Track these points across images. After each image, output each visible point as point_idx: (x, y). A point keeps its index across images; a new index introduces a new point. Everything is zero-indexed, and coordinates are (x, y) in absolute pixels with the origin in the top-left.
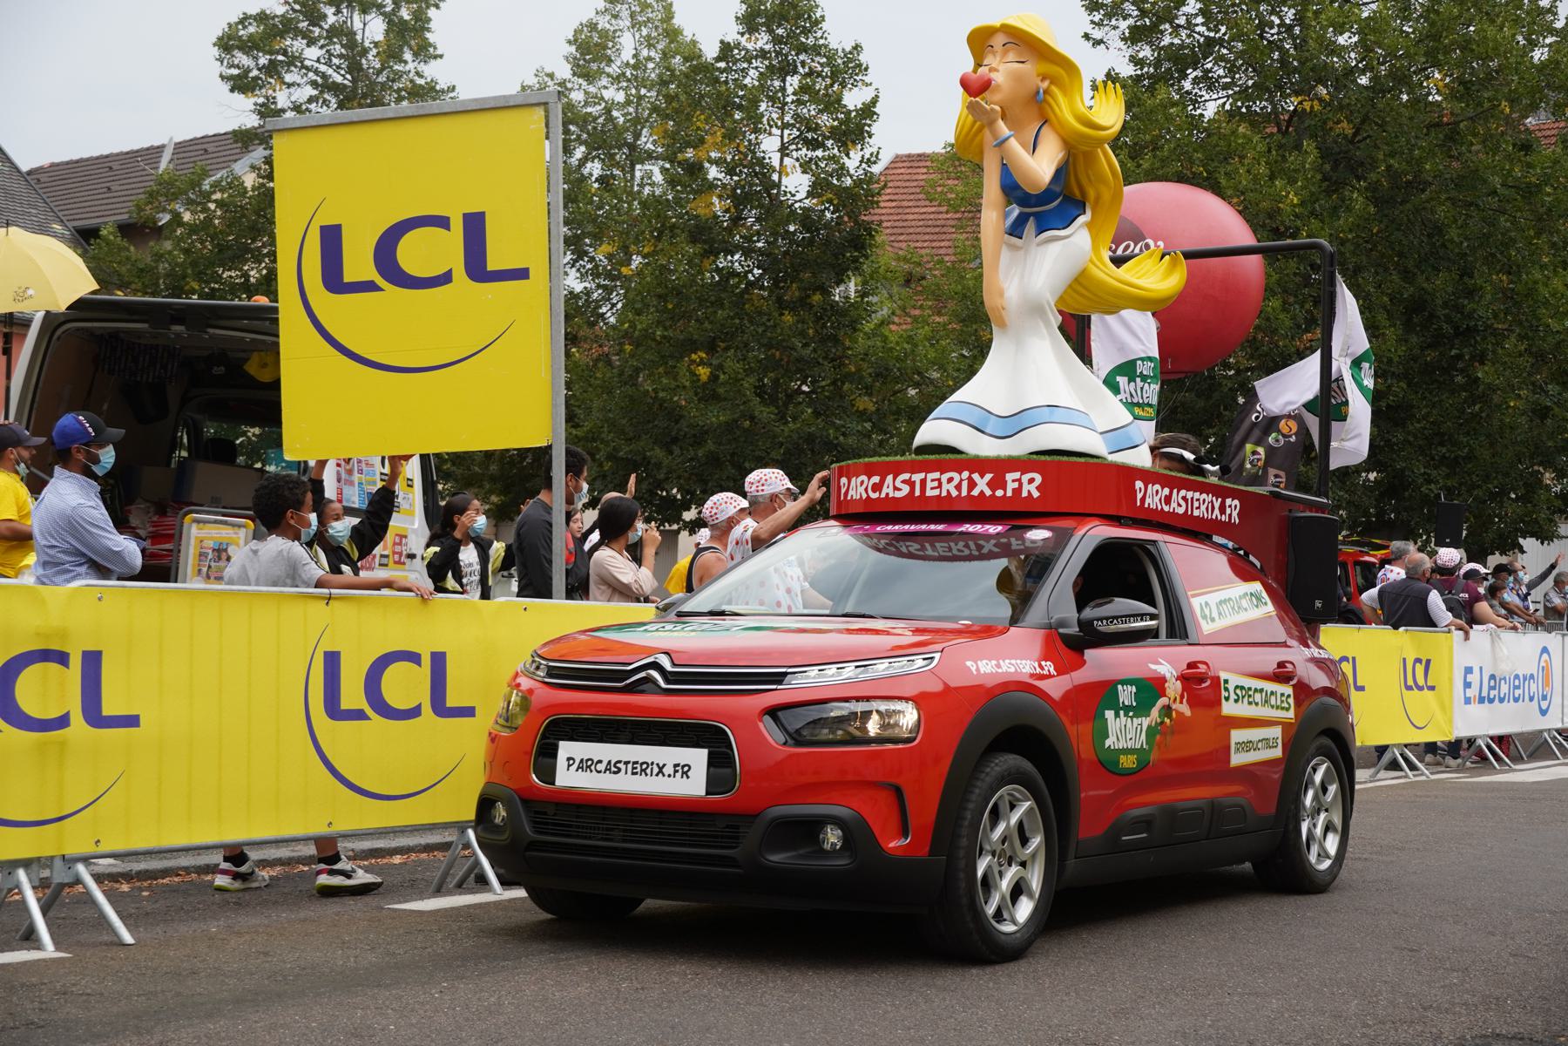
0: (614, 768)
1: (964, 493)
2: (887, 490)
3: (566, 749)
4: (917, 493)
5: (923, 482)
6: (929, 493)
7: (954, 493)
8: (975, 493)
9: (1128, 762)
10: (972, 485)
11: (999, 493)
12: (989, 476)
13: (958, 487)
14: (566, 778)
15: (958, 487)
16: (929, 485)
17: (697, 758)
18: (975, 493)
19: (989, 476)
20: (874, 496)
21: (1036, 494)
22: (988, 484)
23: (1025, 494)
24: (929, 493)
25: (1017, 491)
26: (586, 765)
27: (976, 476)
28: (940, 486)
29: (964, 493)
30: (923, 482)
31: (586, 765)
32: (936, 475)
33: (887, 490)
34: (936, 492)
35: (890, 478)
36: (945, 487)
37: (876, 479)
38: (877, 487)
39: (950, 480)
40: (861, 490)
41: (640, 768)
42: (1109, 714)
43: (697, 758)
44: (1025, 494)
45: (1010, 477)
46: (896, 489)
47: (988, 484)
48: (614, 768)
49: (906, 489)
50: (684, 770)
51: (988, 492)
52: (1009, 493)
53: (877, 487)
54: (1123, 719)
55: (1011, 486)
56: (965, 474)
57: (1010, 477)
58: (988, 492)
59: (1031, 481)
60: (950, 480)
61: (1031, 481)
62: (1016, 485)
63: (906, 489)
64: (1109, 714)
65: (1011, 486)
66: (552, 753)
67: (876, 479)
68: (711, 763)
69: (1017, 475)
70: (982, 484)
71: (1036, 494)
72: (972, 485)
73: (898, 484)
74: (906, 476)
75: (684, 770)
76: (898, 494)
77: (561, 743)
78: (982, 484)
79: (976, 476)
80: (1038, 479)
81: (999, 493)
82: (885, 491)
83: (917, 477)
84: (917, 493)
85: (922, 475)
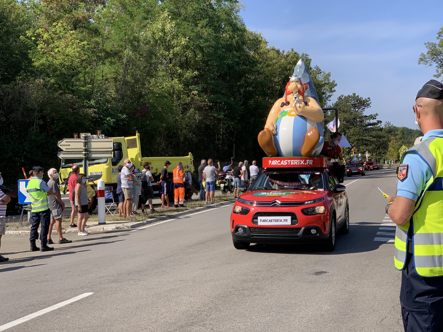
0: (271, 221)
2: (282, 163)
3: (260, 218)
5: (290, 162)
6: (292, 164)
10: (300, 162)
13: (298, 163)
14: (260, 223)
15: (298, 163)
17: (289, 218)
24: (292, 164)
25: (309, 163)
26: (264, 221)
30: (290, 162)
31: (264, 221)
35: (283, 161)
36: (295, 163)
37: (279, 161)
41: (277, 221)
43: (289, 218)
45: (307, 161)
48: (271, 221)
50: (286, 220)
53: (279, 163)
55: (308, 162)
57: (307, 161)
63: (286, 163)
65: (308, 162)
66: (257, 219)
67: (279, 161)
68: (292, 219)
72: (300, 162)
75: (286, 220)
77: (259, 217)
78: (302, 162)
80: (312, 161)
83: (289, 161)
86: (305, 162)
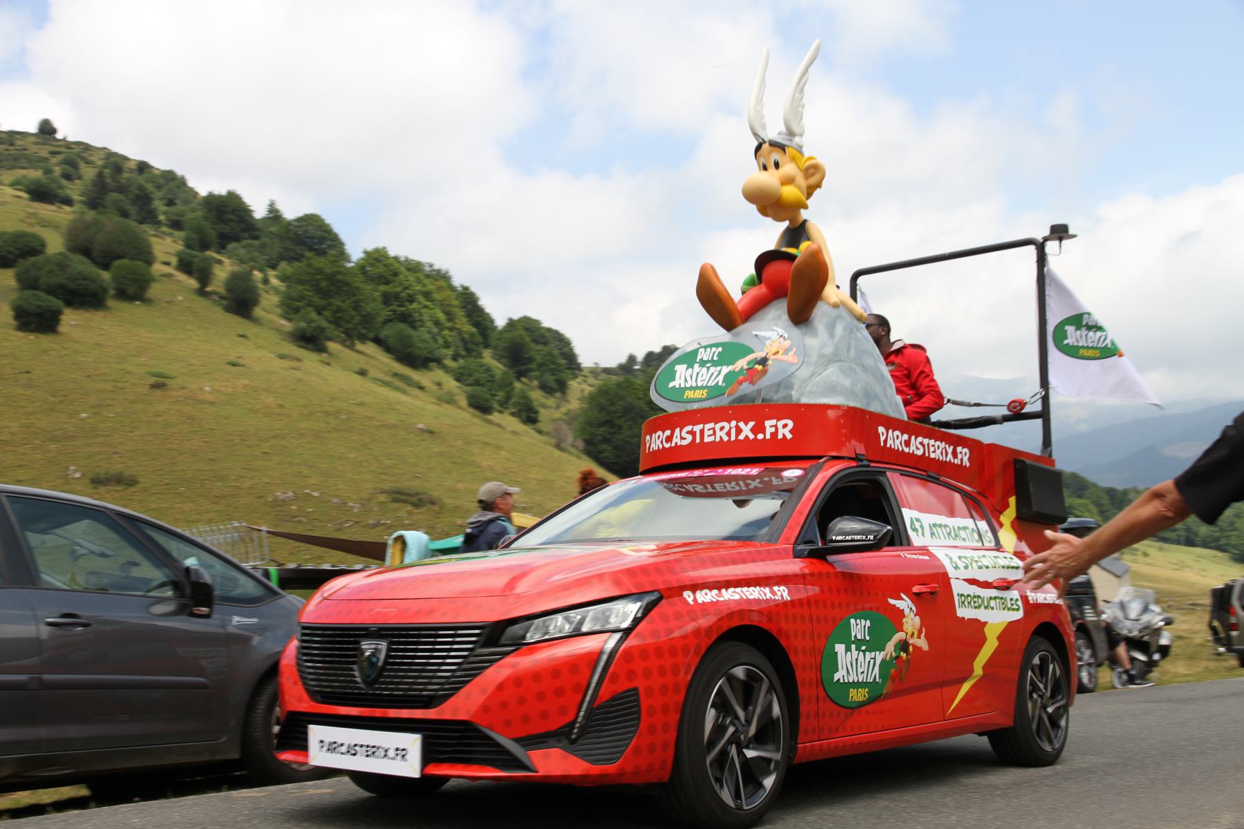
1: (733, 438)
2: (676, 440)
4: (698, 440)
5: (702, 432)
7: (726, 439)
8: (741, 437)
9: (858, 695)
10: (739, 431)
11: (760, 436)
12: (751, 424)
13: (728, 434)
15: (728, 434)
16: (707, 433)
18: (741, 437)
19: (751, 424)
20: (667, 446)
21: (789, 436)
22: (751, 430)
23: (780, 436)
24: (707, 439)
25: (774, 435)
27: (741, 424)
28: (714, 433)
29: (733, 438)
30: (702, 432)
32: (711, 425)
33: (676, 440)
34: (712, 439)
35: (677, 430)
36: (719, 434)
37: (668, 433)
38: (669, 439)
39: (722, 428)
40: (659, 442)
42: (840, 648)
44: (780, 436)
45: (768, 423)
46: (682, 438)
47: (751, 430)
49: (689, 438)
51: (751, 436)
52: (768, 437)
53: (669, 439)
54: (855, 653)
55: (769, 431)
56: (734, 423)
57: (768, 423)
58: (751, 436)
59: (785, 426)
60: (722, 428)
61: (785, 426)
62: (773, 430)
63: (689, 438)
64: (840, 648)
65: (769, 431)
67: (668, 433)
69: (773, 422)
70: (747, 430)
71: (789, 436)
72: (739, 431)
73: (684, 435)
74: (689, 428)
76: (684, 443)
78: (747, 430)
79: (741, 424)
80: (791, 424)
81: (760, 436)
82: (674, 440)
83: (697, 428)
84: (698, 440)
85: (701, 426)
86: (758, 429)
